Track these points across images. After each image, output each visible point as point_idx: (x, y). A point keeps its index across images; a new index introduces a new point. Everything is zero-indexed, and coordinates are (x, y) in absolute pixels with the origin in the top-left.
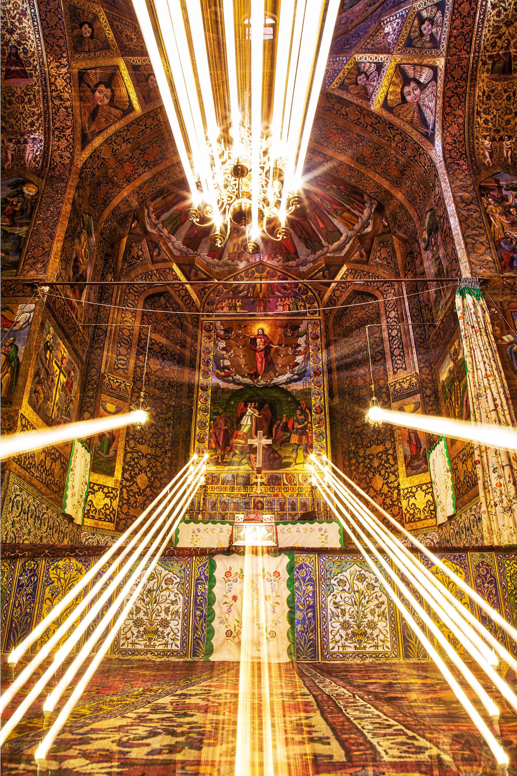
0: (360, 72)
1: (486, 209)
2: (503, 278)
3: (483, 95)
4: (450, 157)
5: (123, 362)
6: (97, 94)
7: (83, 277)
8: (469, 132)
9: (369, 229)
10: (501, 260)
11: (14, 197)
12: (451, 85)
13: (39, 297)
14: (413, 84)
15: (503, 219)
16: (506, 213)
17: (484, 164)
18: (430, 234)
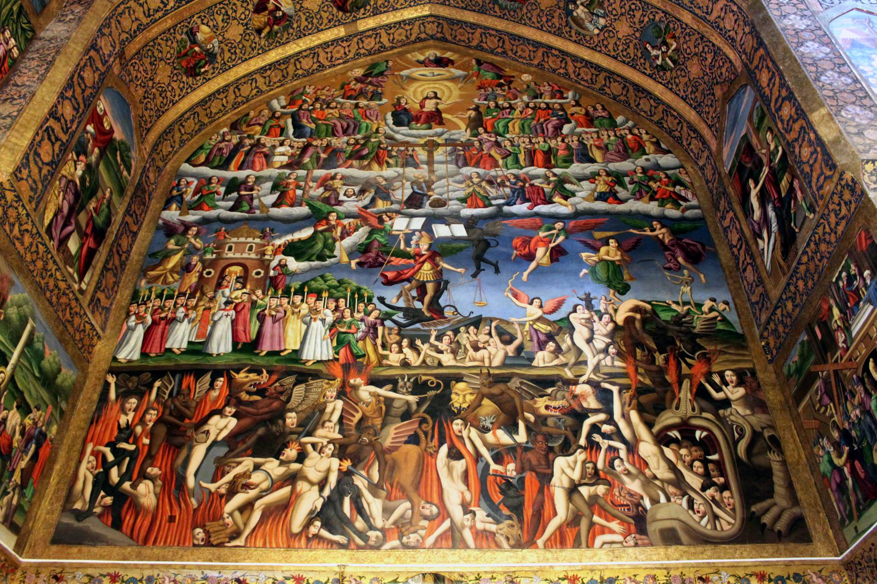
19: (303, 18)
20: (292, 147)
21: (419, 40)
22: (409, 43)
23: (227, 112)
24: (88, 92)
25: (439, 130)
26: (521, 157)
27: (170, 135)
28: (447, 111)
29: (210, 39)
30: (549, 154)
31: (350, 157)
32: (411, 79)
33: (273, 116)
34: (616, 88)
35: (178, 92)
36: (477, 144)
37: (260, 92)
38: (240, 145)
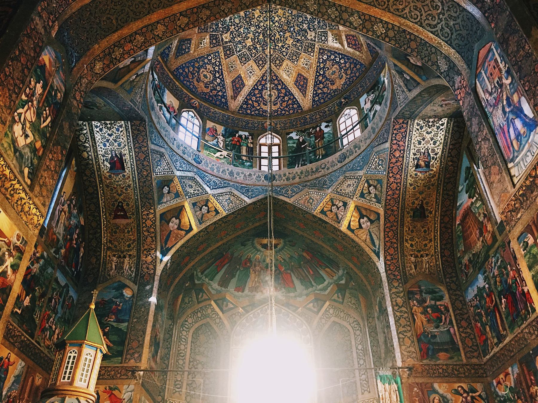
0: (333, 205)
1: (412, 309)
2: (422, 365)
3: (409, 230)
4: (390, 270)
5: (178, 386)
6: (171, 224)
7: (159, 344)
8: (401, 252)
9: (343, 282)
10: (421, 350)
11: (117, 298)
12: (388, 225)
13: (137, 380)
14: (365, 219)
15: (423, 317)
16: (425, 312)
17: (411, 274)
18: (380, 311)
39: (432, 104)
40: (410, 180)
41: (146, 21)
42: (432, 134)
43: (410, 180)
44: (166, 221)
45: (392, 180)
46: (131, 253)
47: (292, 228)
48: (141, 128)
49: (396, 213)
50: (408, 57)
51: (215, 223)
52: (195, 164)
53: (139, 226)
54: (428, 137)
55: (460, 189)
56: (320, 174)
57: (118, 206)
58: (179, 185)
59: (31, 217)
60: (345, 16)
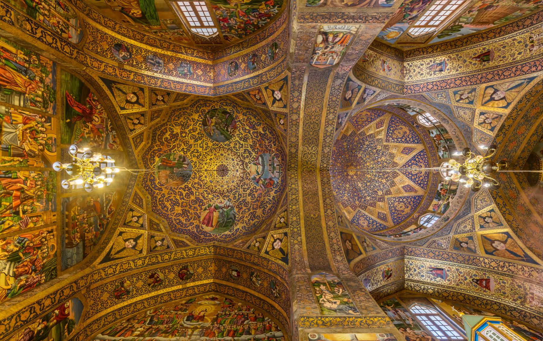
0: (484, 122)
3: (501, 60)
12: (497, 77)
14: (494, 96)
19: (167, 281)
20: (144, 328)
21: (209, 291)
22: (204, 292)
23: (129, 315)
24: (63, 297)
25: (200, 323)
26: (225, 333)
27: (99, 321)
28: (207, 316)
29: (130, 286)
30: (236, 331)
31: (163, 333)
32: (200, 304)
33: (145, 317)
34: (266, 307)
35: (109, 304)
36: (211, 328)
37: (146, 308)
38: (126, 327)
39: (387, 76)
40: (454, 72)
41: (324, 229)
42: (415, 68)
43: (454, 72)
44: (494, 251)
45: (452, 85)
46: (528, 287)
47: (519, 152)
48: (410, 249)
49: (484, 75)
50: (348, 98)
51: (503, 214)
52: (448, 221)
53: (498, 273)
54: (417, 70)
55: (460, 36)
56: (459, 134)
57: (476, 282)
58: (461, 235)
59: (378, 323)
60: (328, 134)
